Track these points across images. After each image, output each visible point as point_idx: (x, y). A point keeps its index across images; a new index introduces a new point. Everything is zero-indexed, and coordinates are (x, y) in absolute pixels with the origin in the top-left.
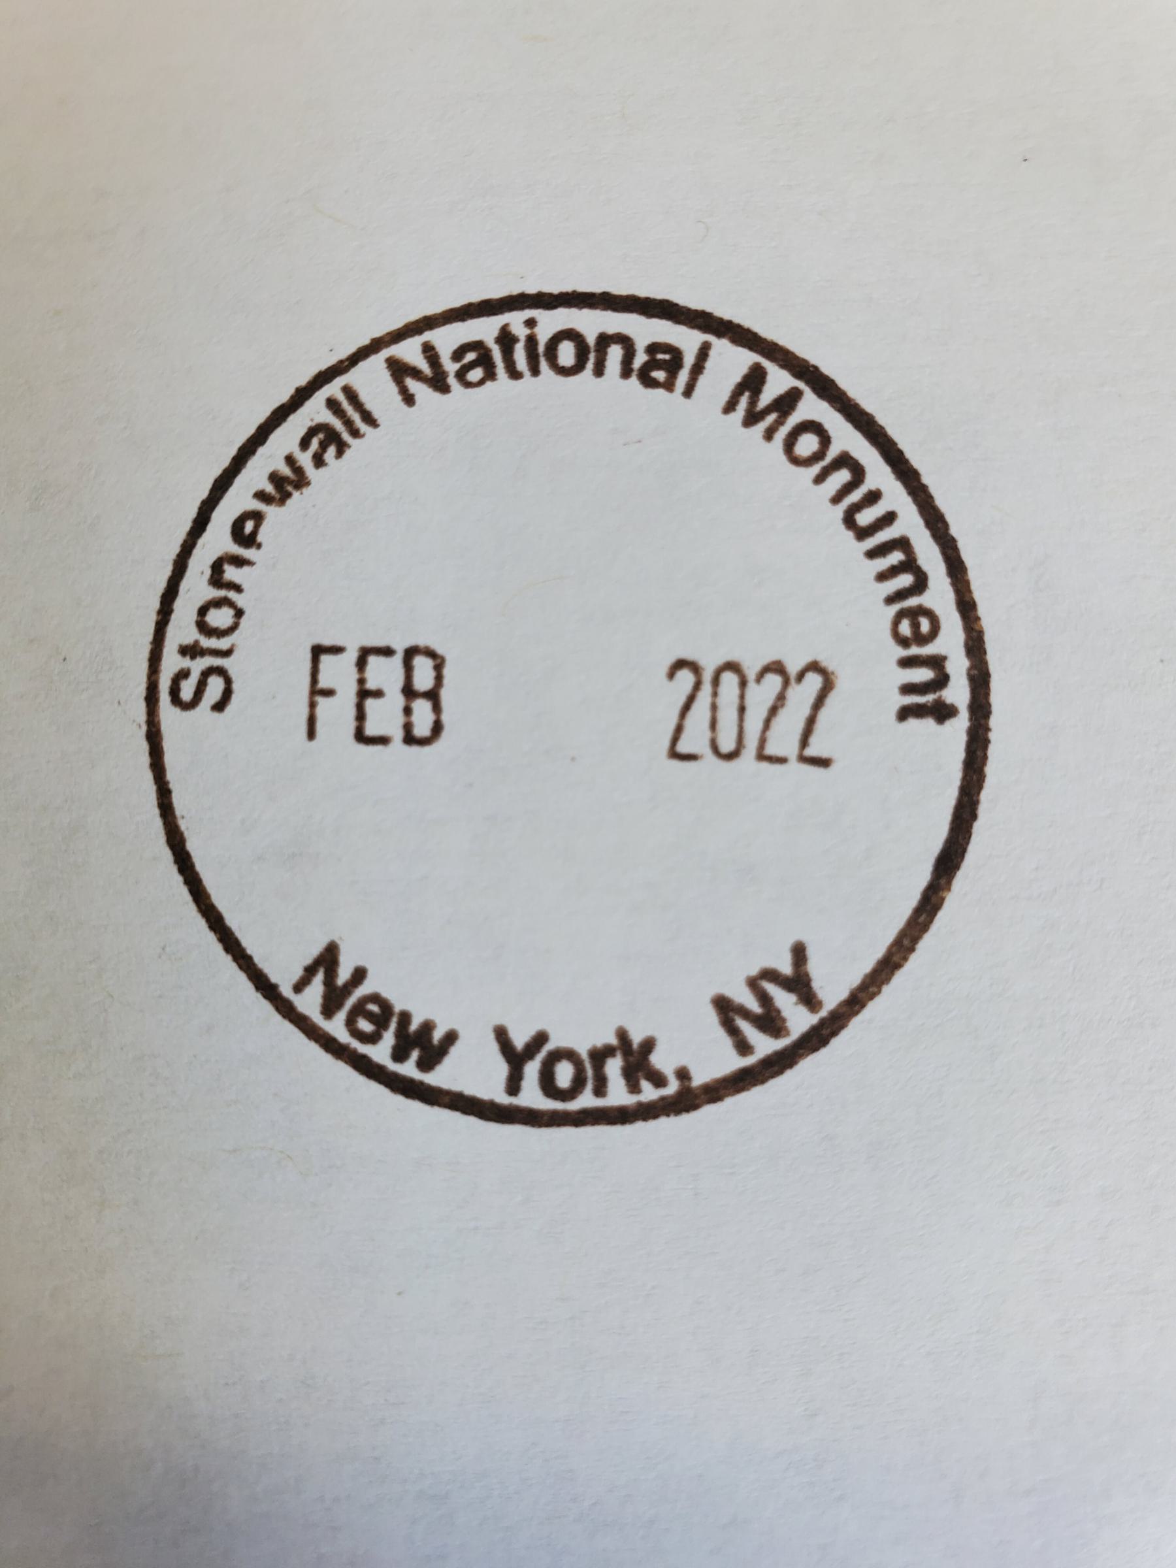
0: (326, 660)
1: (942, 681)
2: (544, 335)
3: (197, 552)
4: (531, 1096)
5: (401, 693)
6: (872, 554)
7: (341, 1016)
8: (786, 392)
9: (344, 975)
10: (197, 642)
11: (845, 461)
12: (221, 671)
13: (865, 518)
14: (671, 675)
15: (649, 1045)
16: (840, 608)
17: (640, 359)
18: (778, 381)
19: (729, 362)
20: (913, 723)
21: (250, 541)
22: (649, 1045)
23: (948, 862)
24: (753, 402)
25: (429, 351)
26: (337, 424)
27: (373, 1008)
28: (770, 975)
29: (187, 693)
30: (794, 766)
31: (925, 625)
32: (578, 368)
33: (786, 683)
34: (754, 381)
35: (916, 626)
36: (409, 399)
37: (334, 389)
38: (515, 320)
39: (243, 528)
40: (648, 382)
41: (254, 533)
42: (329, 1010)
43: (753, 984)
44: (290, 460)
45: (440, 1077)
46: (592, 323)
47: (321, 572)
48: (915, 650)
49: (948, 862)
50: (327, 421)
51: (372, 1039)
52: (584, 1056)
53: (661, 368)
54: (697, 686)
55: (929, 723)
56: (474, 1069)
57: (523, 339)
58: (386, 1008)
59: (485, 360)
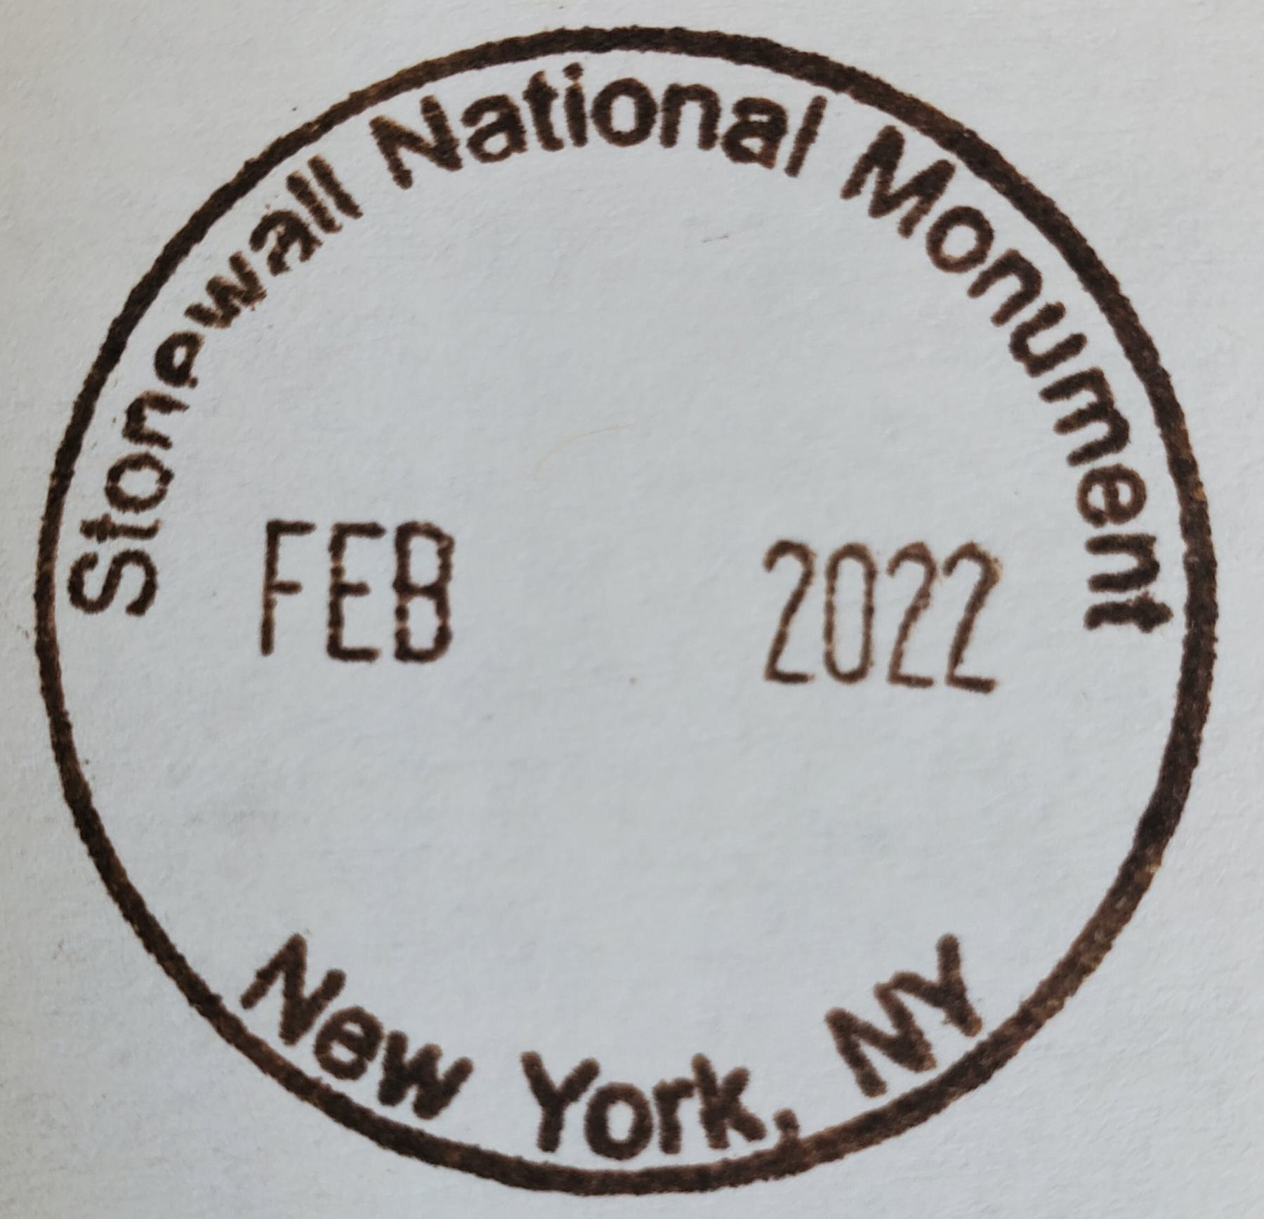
0: (287, 542)
1: (1148, 571)
2: (591, 88)
3: (107, 391)
4: (574, 1151)
5: (397, 589)
6: (1051, 394)
7: (308, 1040)
8: (929, 167)
9: (312, 983)
10: (106, 518)
11: (1012, 263)
12: (140, 558)
13: (1041, 343)
14: (770, 563)
15: (738, 1081)
16: (1005, 470)
17: (727, 121)
18: (920, 152)
19: (853, 125)
20: (1108, 630)
21: (181, 376)
22: (738, 1081)
23: (1158, 824)
24: (884, 181)
25: (431, 109)
26: (303, 213)
27: (354, 1028)
28: (908, 982)
29: (93, 585)
30: (942, 689)
31: (1125, 494)
32: (640, 133)
33: (931, 574)
34: (885, 152)
35: (1112, 495)
36: (403, 177)
37: (298, 163)
38: (553, 67)
39: (171, 357)
40: (737, 153)
41: (187, 365)
42: (291, 1033)
43: (884, 995)
44: (237, 262)
45: (446, 1126)
46: (658, 71)
47: (276, 422)
48: (1110, 529)
49: (1158, 824)
50: (289, 208)
51: (352, 1072)
52: (649, 1095)
53: (755, 134)
54: (807, 578)
55: (1130, 632)
56: (494, 1114)
57: (562, 93)
58: (371, 1027)
59: (510, 123)
